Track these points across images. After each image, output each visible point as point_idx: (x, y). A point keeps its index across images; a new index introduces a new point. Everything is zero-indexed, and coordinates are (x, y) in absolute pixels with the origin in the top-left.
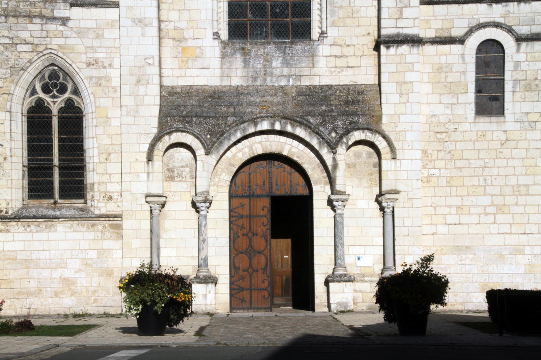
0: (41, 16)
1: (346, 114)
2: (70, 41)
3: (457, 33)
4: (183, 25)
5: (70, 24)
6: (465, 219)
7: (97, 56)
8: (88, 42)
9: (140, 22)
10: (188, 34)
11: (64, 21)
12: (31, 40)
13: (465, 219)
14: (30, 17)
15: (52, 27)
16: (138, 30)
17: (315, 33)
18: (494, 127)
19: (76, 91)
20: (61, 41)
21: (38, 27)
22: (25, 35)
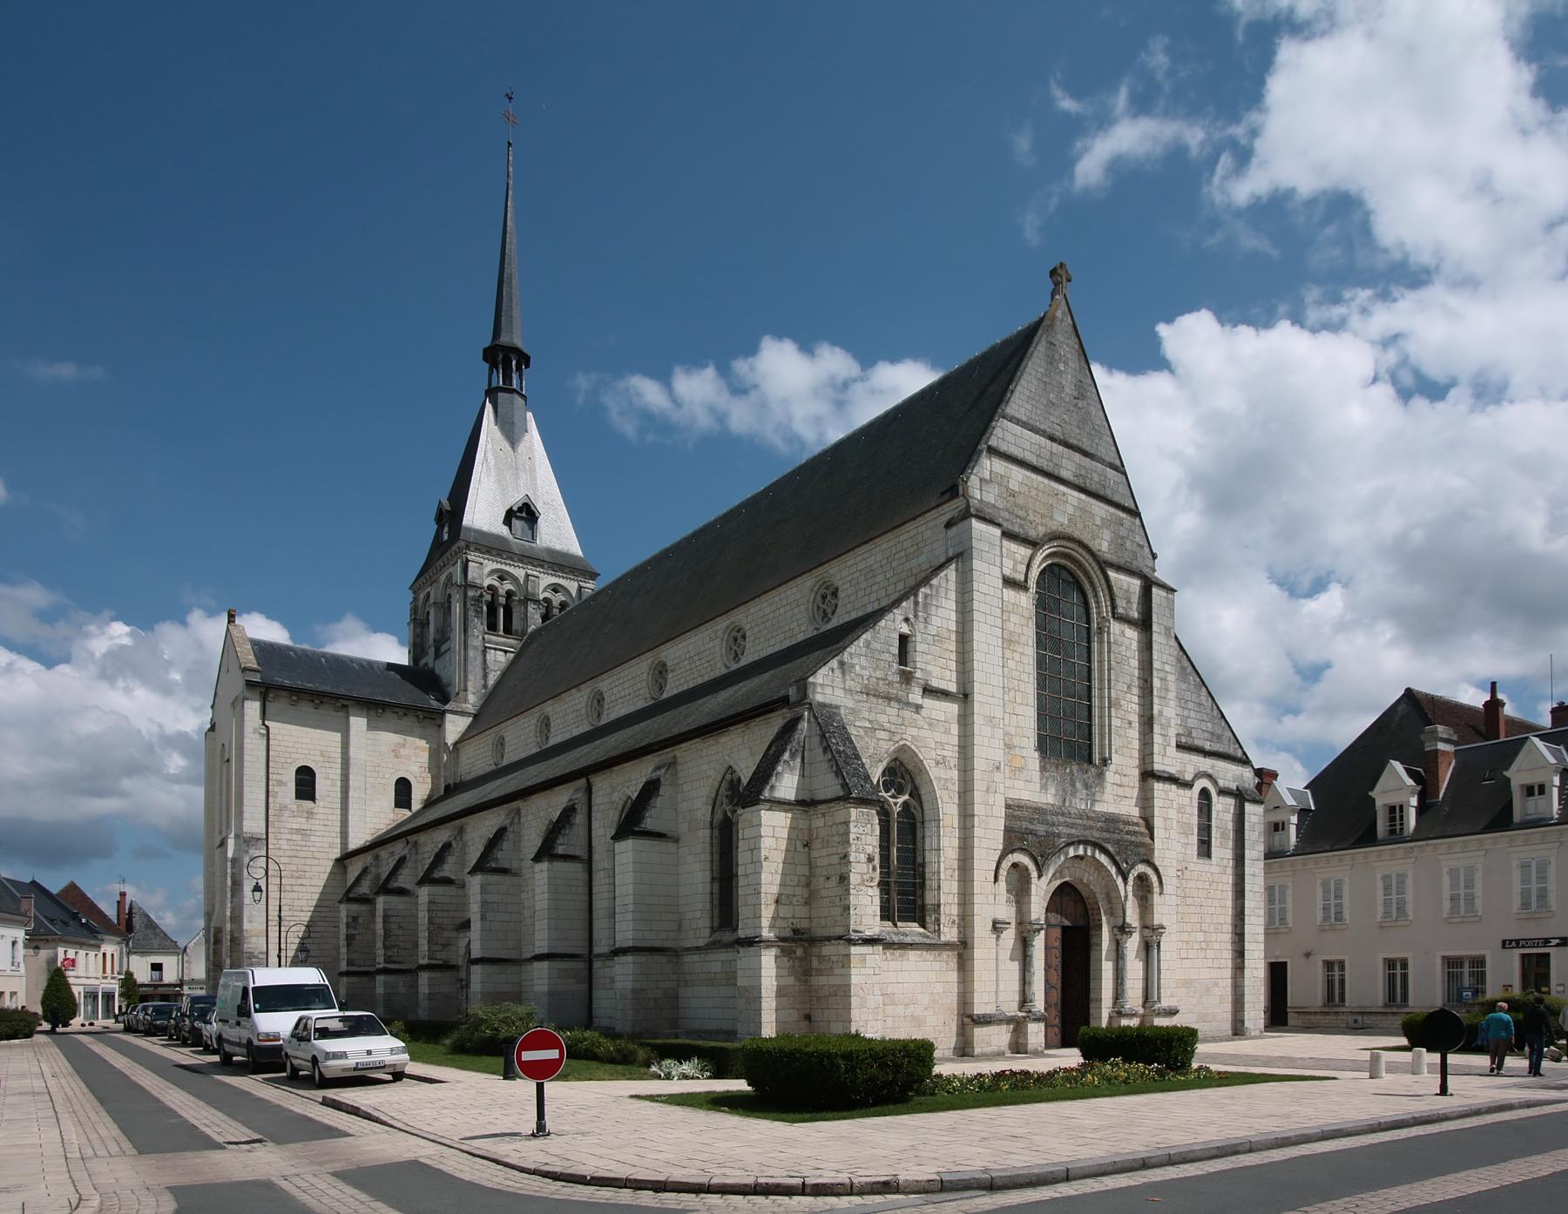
0: (898, 700)
1: (1129, 845)
2: (923, 733)
3: (1188, 777)
4: (1012, 730)
5: (923, 712)
6: (1192, 954)
7: (946, 753)
8: (937, 736)
9: (990, 720)
10: (1016, 741)
11: (918, 708)
12: (887, 725)
13: (1192, 954)
14: (888, 698)
15: (907, 714)
16: (987, 730)
17: (1096, 758)
18: (1207, 868)
19: (915, 794)
20: (914, 731)
21: (895, 712)
22: (883, 719)
